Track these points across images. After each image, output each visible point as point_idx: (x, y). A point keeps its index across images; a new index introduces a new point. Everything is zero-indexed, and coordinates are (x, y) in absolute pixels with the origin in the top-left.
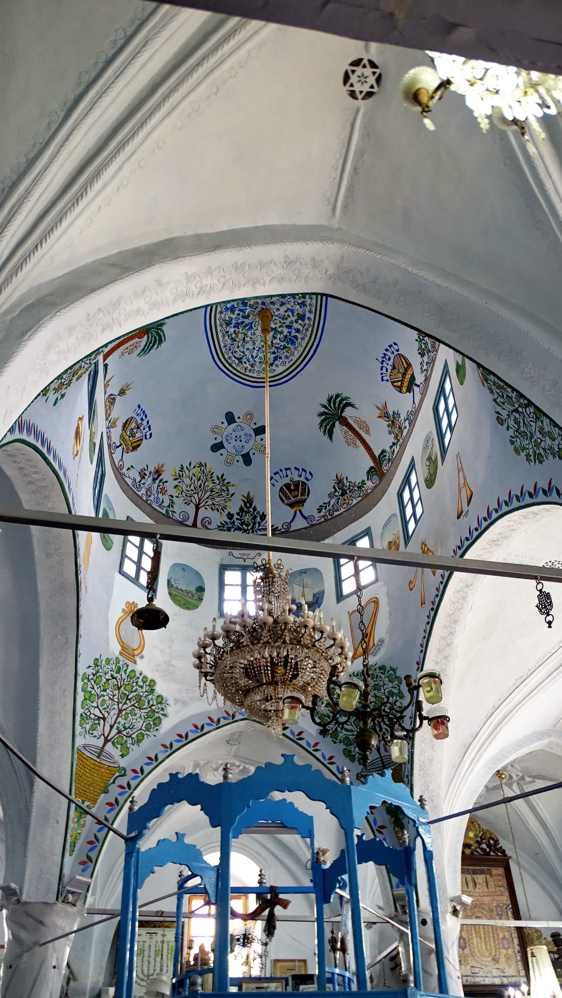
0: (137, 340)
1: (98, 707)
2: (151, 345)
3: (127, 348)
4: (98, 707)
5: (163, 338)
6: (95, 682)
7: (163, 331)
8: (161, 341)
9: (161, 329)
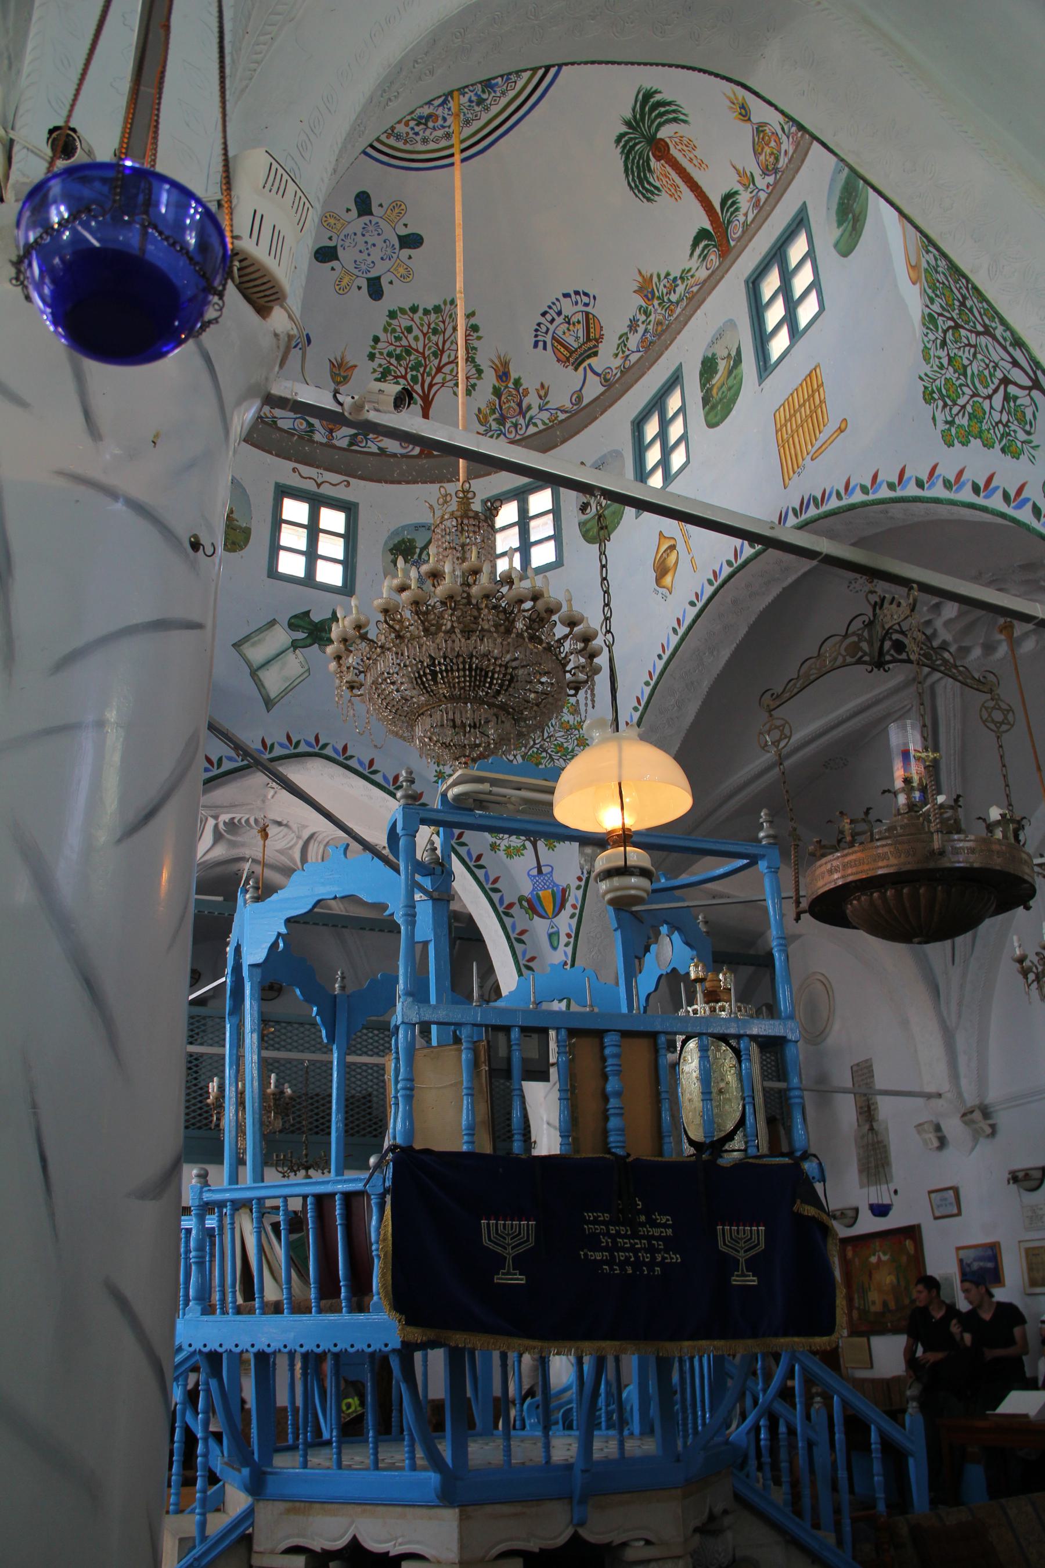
0: (673, 151)
1: (990, 397)
2: (662, 109)
3: (691, 160)
4: (990, 397)
5: (640, 97)
6: (955, 404)
7: (634, 110)
8: (648, 95)
9: (635, 117)
